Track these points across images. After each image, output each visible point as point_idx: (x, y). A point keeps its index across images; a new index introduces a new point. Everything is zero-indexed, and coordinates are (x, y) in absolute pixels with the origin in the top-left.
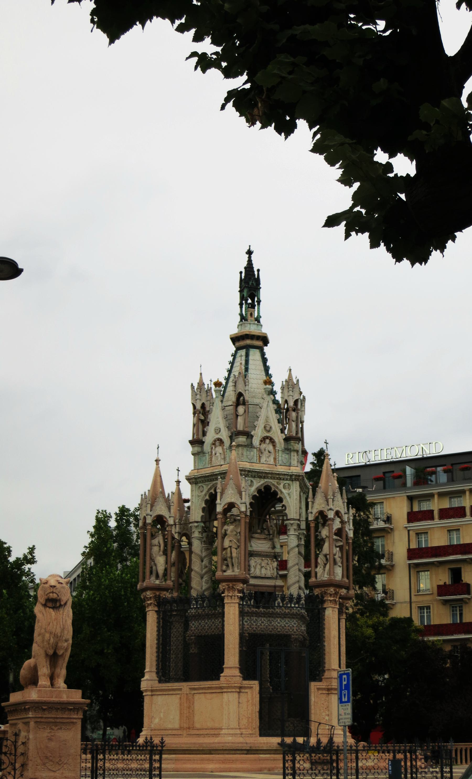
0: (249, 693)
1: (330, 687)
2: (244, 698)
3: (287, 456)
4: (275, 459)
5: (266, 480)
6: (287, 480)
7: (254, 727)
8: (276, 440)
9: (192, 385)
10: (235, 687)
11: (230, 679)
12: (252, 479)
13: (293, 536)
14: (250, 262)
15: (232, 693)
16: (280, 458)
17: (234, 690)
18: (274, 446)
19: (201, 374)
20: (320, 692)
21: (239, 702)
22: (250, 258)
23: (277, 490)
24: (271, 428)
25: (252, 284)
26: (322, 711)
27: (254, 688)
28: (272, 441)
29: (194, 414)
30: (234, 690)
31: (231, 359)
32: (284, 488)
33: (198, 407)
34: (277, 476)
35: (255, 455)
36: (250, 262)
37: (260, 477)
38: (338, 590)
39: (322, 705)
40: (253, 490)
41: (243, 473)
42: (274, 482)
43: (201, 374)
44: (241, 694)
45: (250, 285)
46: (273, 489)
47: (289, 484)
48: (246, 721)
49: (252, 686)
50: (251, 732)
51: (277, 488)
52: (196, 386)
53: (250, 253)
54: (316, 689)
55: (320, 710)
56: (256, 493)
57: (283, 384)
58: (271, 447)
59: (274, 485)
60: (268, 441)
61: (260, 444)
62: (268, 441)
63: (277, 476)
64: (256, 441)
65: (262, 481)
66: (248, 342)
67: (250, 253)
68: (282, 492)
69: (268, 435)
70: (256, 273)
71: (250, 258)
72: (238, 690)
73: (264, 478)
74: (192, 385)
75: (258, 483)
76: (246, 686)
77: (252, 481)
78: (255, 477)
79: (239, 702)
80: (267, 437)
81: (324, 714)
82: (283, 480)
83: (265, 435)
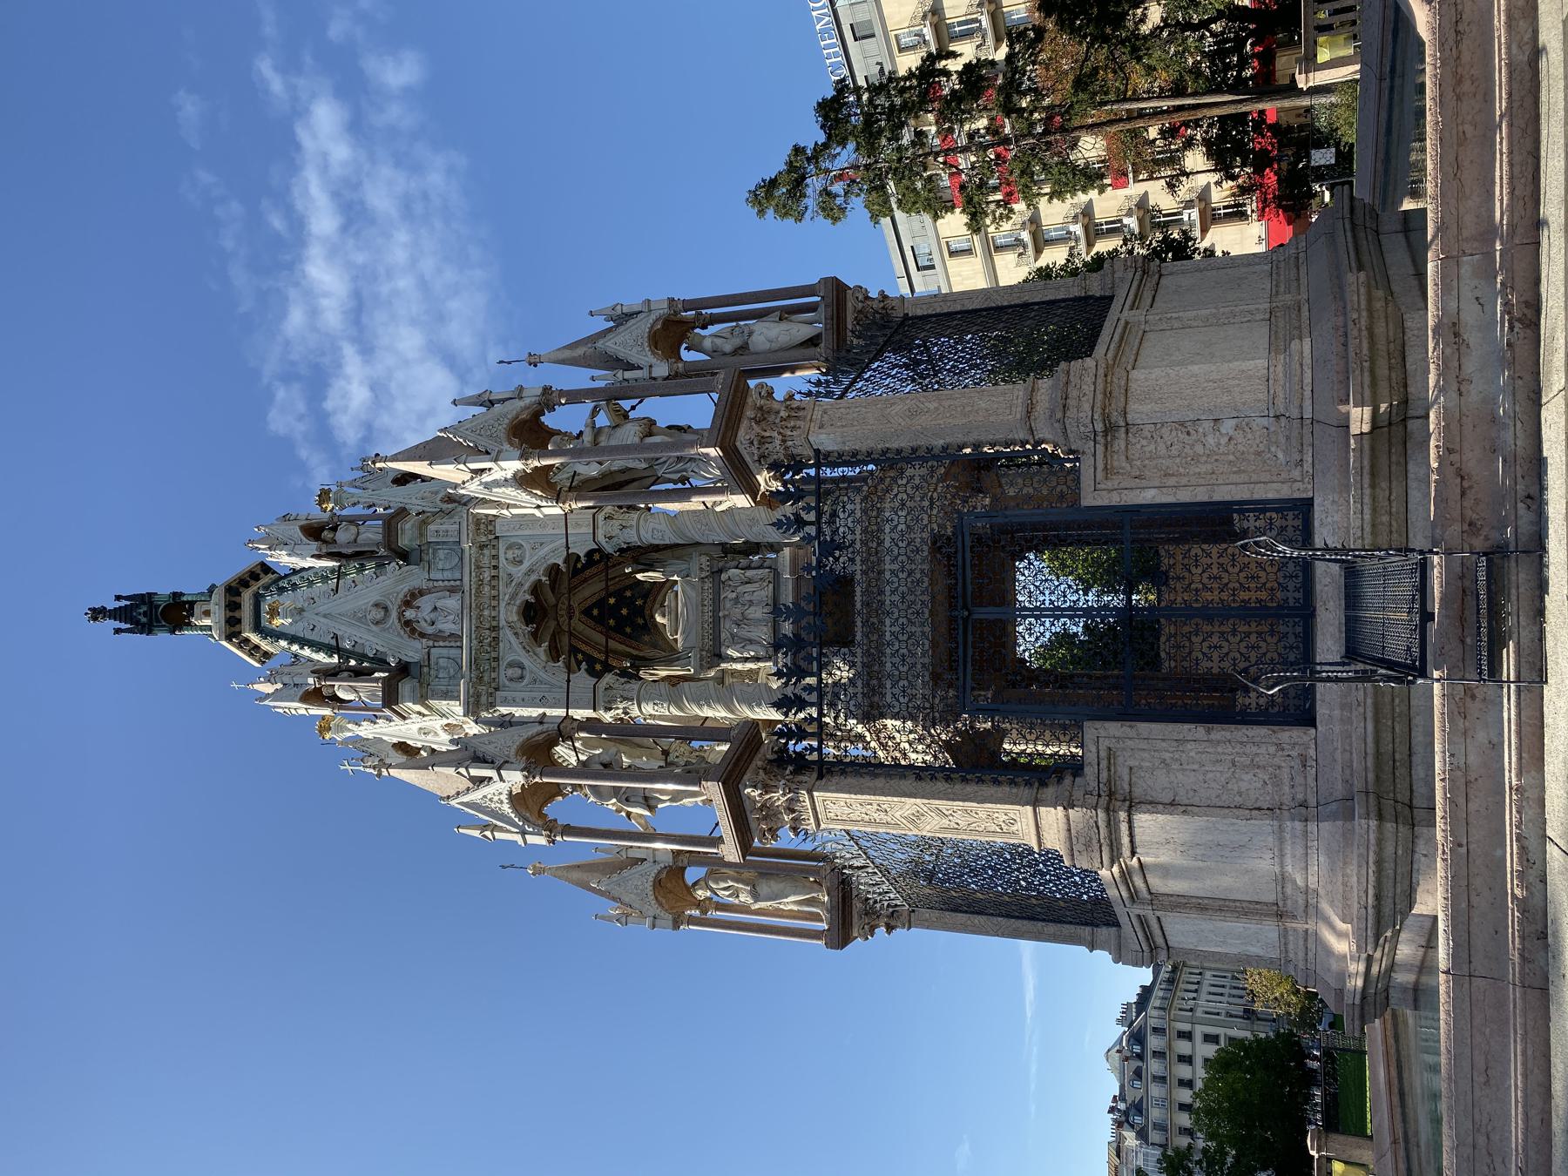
0: (1131, 763)
1: (1099, 427)
2: (1156, 783)
3: (441, 554)
4: (452, 590)
5: (503, 623)
6: (496, 557)
7: (1272, 749)
8: (405, 588)
10: (1112, 826)
11: (1082, 840)
12: (503, 664)
13: (642, 532)
14: (115, 614)
15: (1137, 831)
16: (447, 575)
17: (1124, 827)
18: (421, 593)
20: (1119, 462)
21: (1171, 804)
23: (527, 586)
24: (376, 605)
25: (145, 614)
26: (1199, 449)
27: (1112, 743)
30: (1124, 827)
32: (521, 562)
34: (487, 589)
35: (445, 651)
36: (115, 614)
37: (496, 639)
38: (749, 413)
39: (1174, 451)
40: (535, 661)
41: (483, 699)
42: (505, 592)
44: (1138, 792)
45: (155, 614)
46: (528, 597)
47: (509, 547)
48: (1246, 777)
49: (1103, 754)
50: (1297, 763)
51: (521, 584)
53: (97, 614)
54: (1109, 484)
55: (1195, 458)
56: (542, 650)
58: (425, 603)
59: (513, 597)
60: (410, 614)
61: (422, 635)
62: (410, 614)
63: (487, 589)
64: (412, 651)
65: (507, 634)
67: (97, 614)
68: (530, 571)
69: (394, 614)
70: (124, 603)
72: (1123, 815)
73: (495, 629)
75: (513, 646)
76: (1104, 775)
77: (510, 665)
78: (496, 659)
79: (1171, 804)
80: (401, 614)
81: (1211, 440)
82: (495, 567)
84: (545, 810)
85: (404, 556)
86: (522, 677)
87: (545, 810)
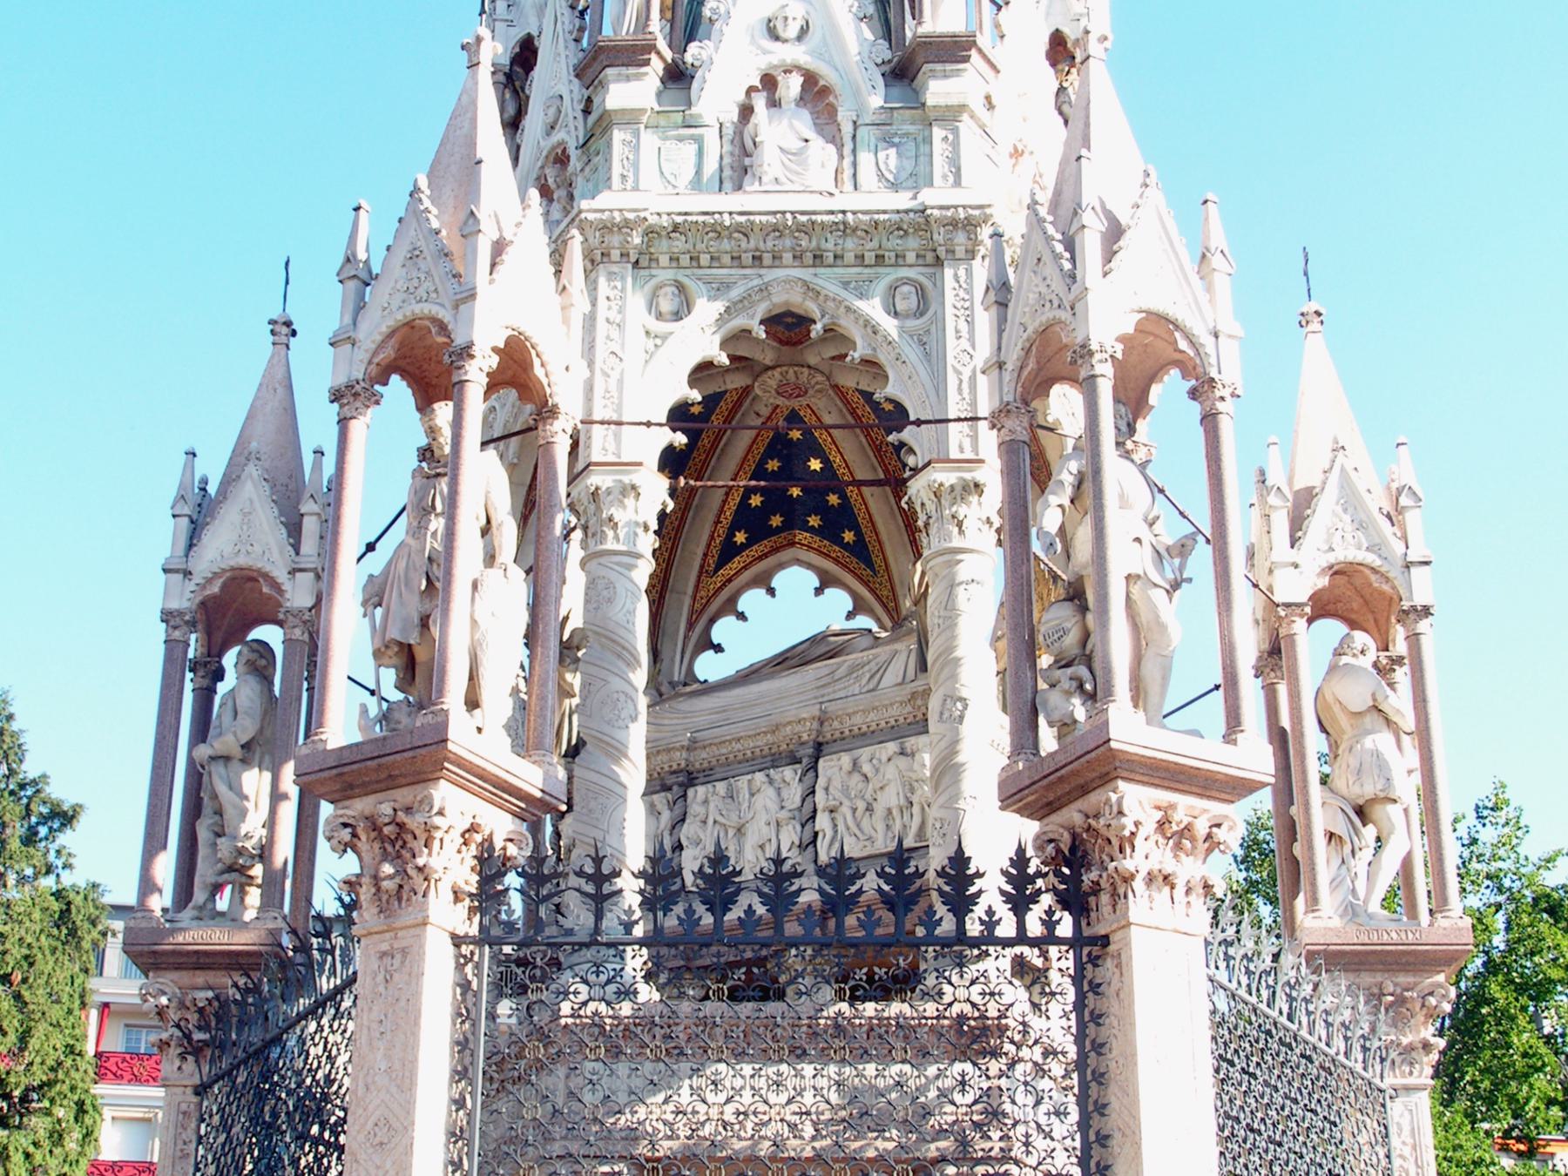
28: (816, 93)
42: (827, 280)
64: (717, 96)
84: (395, 379)
85: (903, 72)
86: (660, 316)
87: (395, 379)
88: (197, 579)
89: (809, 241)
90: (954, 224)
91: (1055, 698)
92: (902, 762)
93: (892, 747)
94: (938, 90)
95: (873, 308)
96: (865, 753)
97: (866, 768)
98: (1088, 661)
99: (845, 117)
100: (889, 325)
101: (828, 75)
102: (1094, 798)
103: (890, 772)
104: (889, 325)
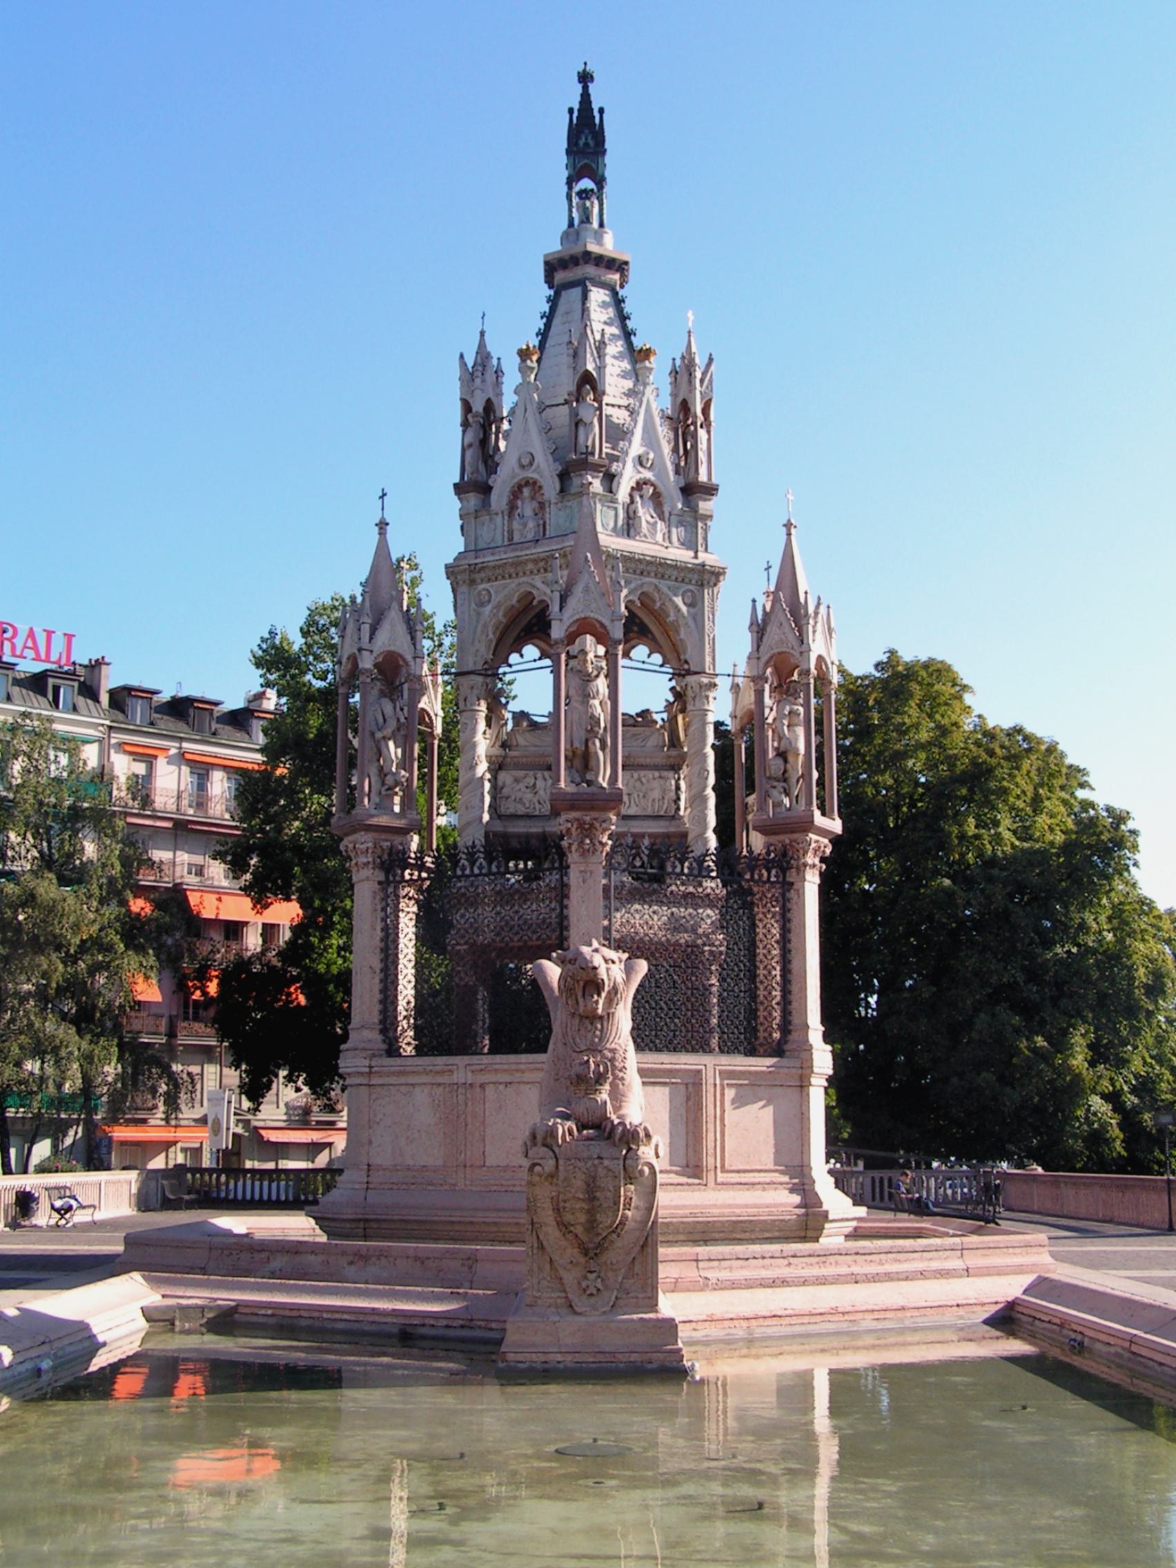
9: (462, 356)
14: (586, 98)
19: (482, 334)
22: (585, 88)
29: (465, 424)
31: (546, 308)
33: (478, 407)
36: (586, 98)
42: (664, 585)
43: (482, 334)
52: (470, 362)
53: (585, 78)
57: (674, 364)
66: (590, 270)
67: (585, 78)
71: (585, 88)
74: (462, 356)
83: (642, 476)
88: (375, 654)
89: (659, 568)
90: (713, 573)
91: (775, 793)
92: (662, 782)
93: (657, 774)
94: (704, 506)
95: (678, 601)
96: (642, 773)
97: (644, 780)
98: (785, 780)
99: (666, 509)
100: (684, 609)
101: (661, 488)
102: (795, 836)
103: (655, 784)
104: (684, 609)
